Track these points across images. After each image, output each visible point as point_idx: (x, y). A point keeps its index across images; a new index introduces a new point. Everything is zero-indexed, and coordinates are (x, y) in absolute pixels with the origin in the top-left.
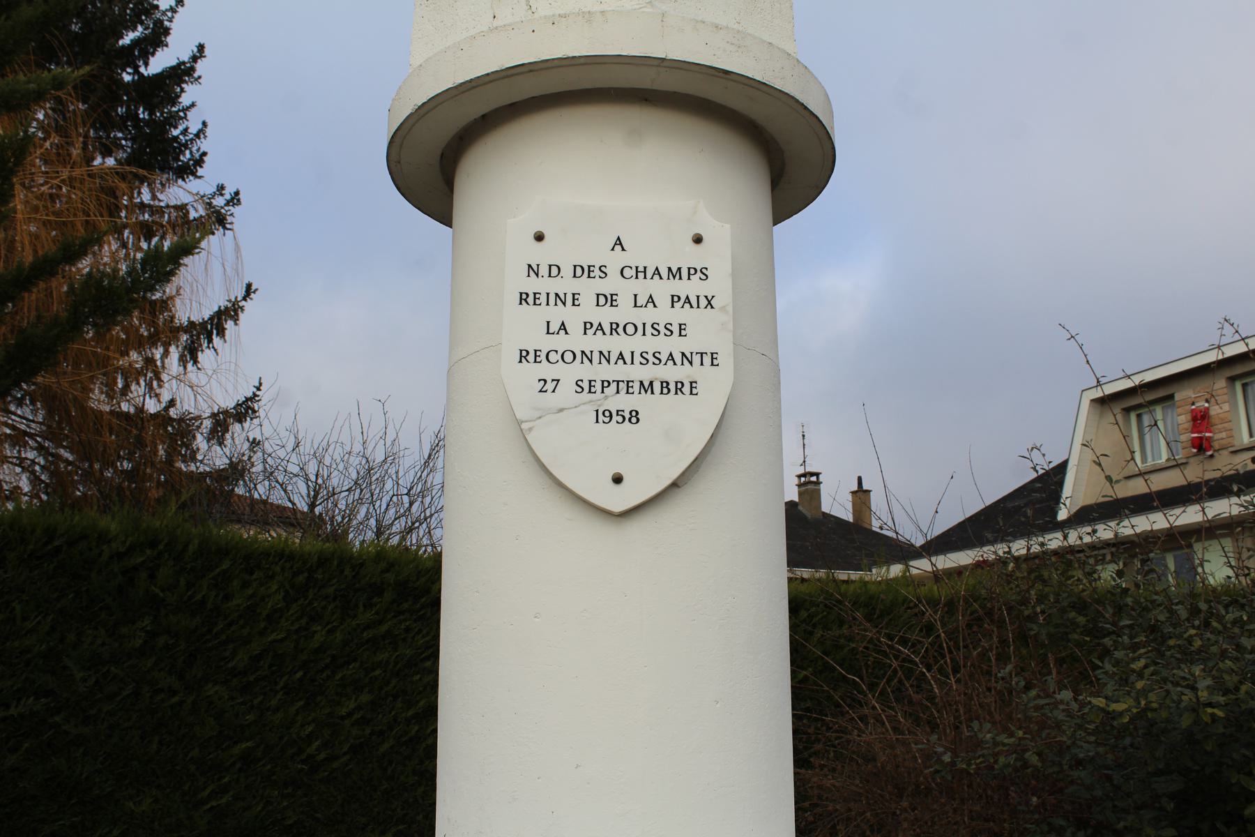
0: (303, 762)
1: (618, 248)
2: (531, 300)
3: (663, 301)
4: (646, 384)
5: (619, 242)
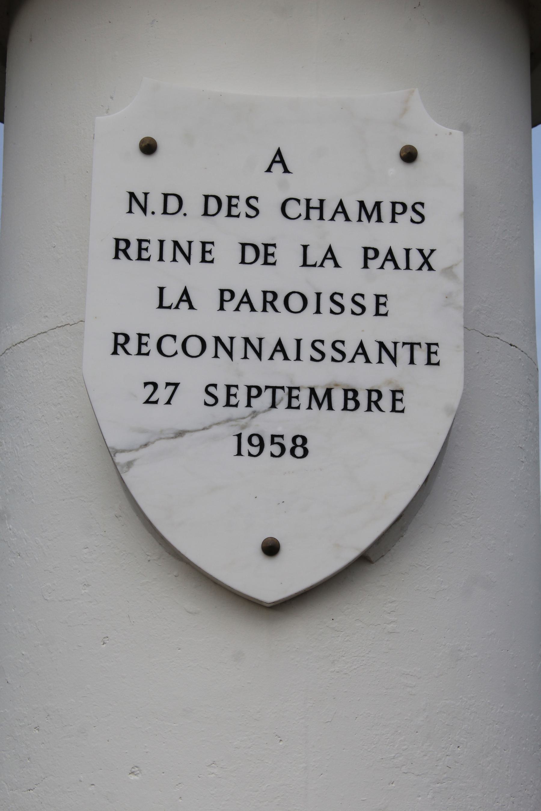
1: (278, 168)
2: (133, 251)
3: (349, 257)
4: (320, 393)
5: (279, 158)
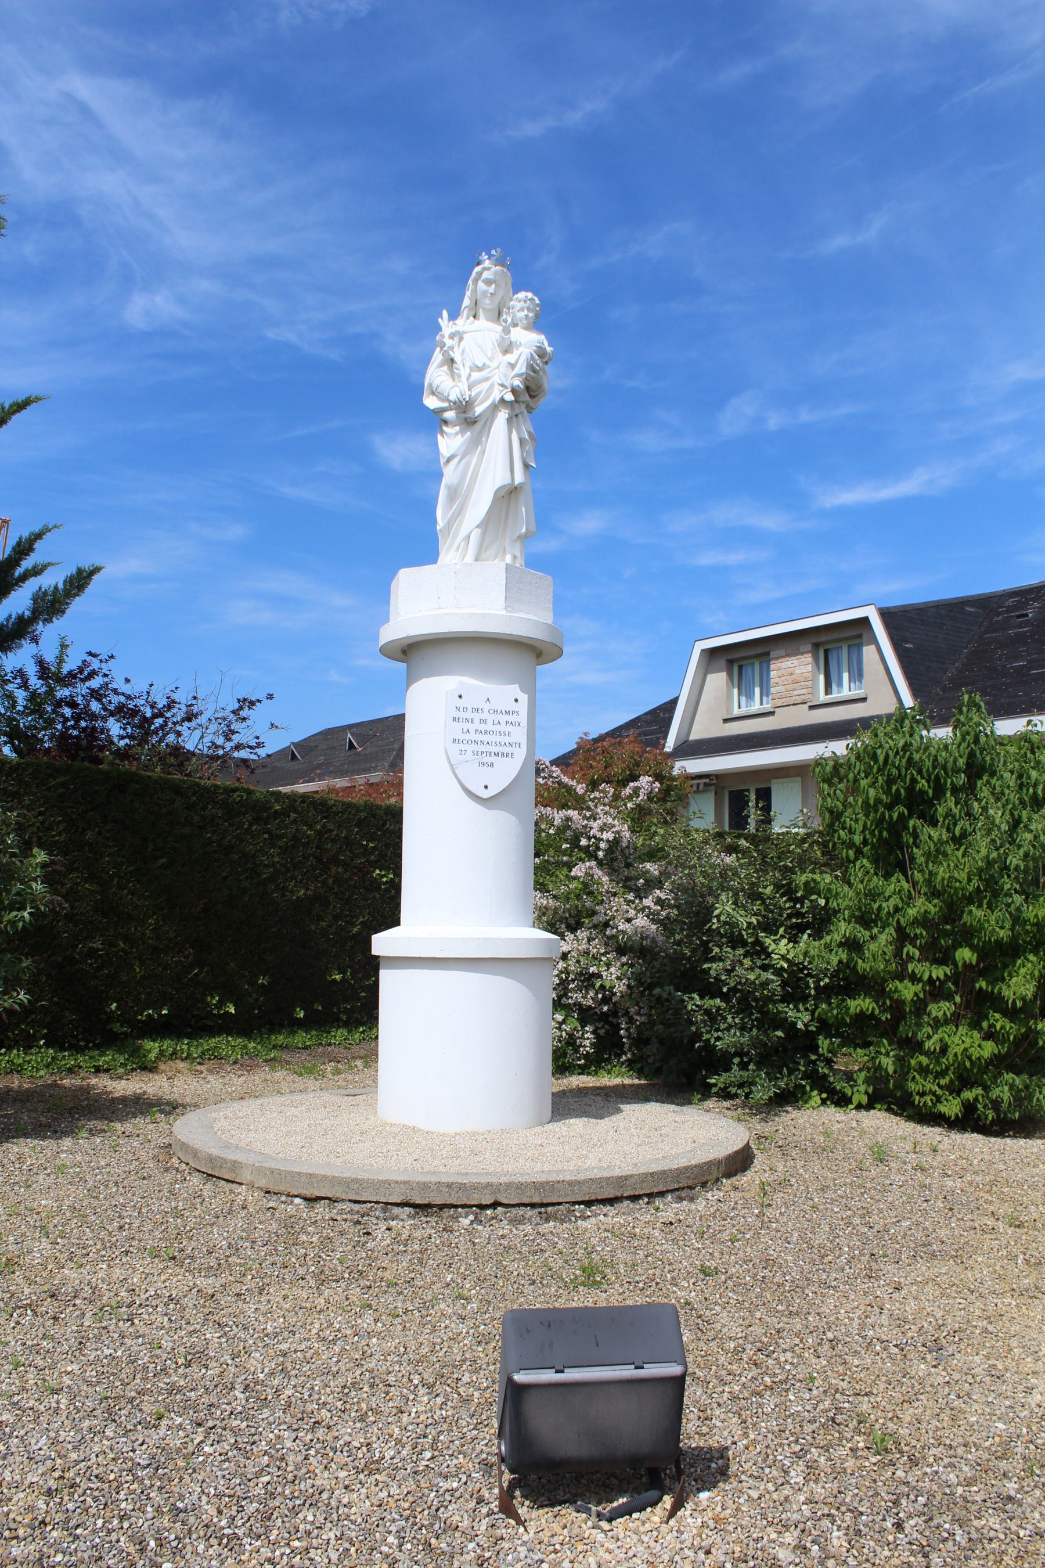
3: (503, 723)
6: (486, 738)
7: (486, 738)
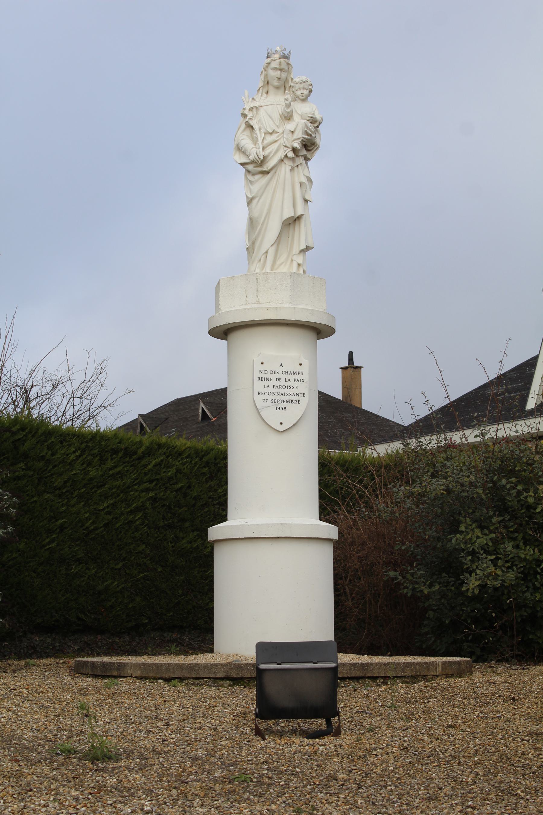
0: (83, 530)
3: (292, 380)
6: (281, 391)
7: (281, 391)
